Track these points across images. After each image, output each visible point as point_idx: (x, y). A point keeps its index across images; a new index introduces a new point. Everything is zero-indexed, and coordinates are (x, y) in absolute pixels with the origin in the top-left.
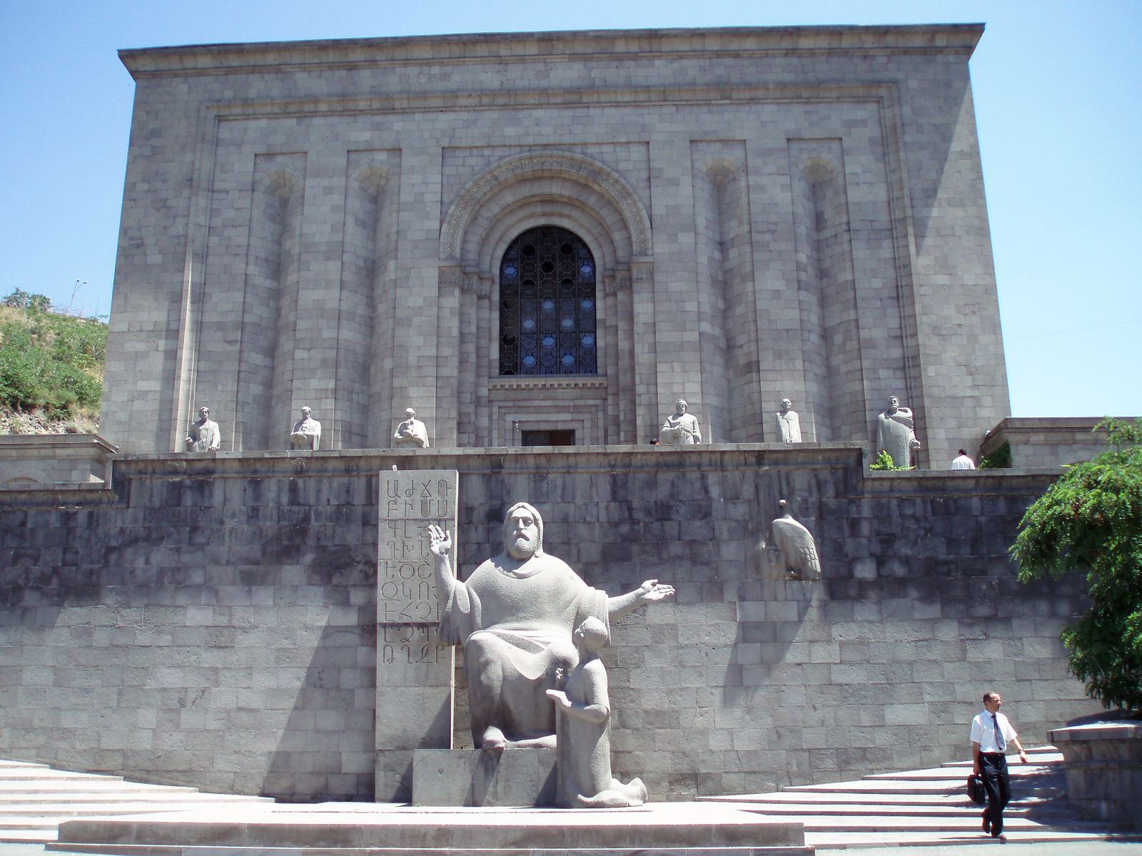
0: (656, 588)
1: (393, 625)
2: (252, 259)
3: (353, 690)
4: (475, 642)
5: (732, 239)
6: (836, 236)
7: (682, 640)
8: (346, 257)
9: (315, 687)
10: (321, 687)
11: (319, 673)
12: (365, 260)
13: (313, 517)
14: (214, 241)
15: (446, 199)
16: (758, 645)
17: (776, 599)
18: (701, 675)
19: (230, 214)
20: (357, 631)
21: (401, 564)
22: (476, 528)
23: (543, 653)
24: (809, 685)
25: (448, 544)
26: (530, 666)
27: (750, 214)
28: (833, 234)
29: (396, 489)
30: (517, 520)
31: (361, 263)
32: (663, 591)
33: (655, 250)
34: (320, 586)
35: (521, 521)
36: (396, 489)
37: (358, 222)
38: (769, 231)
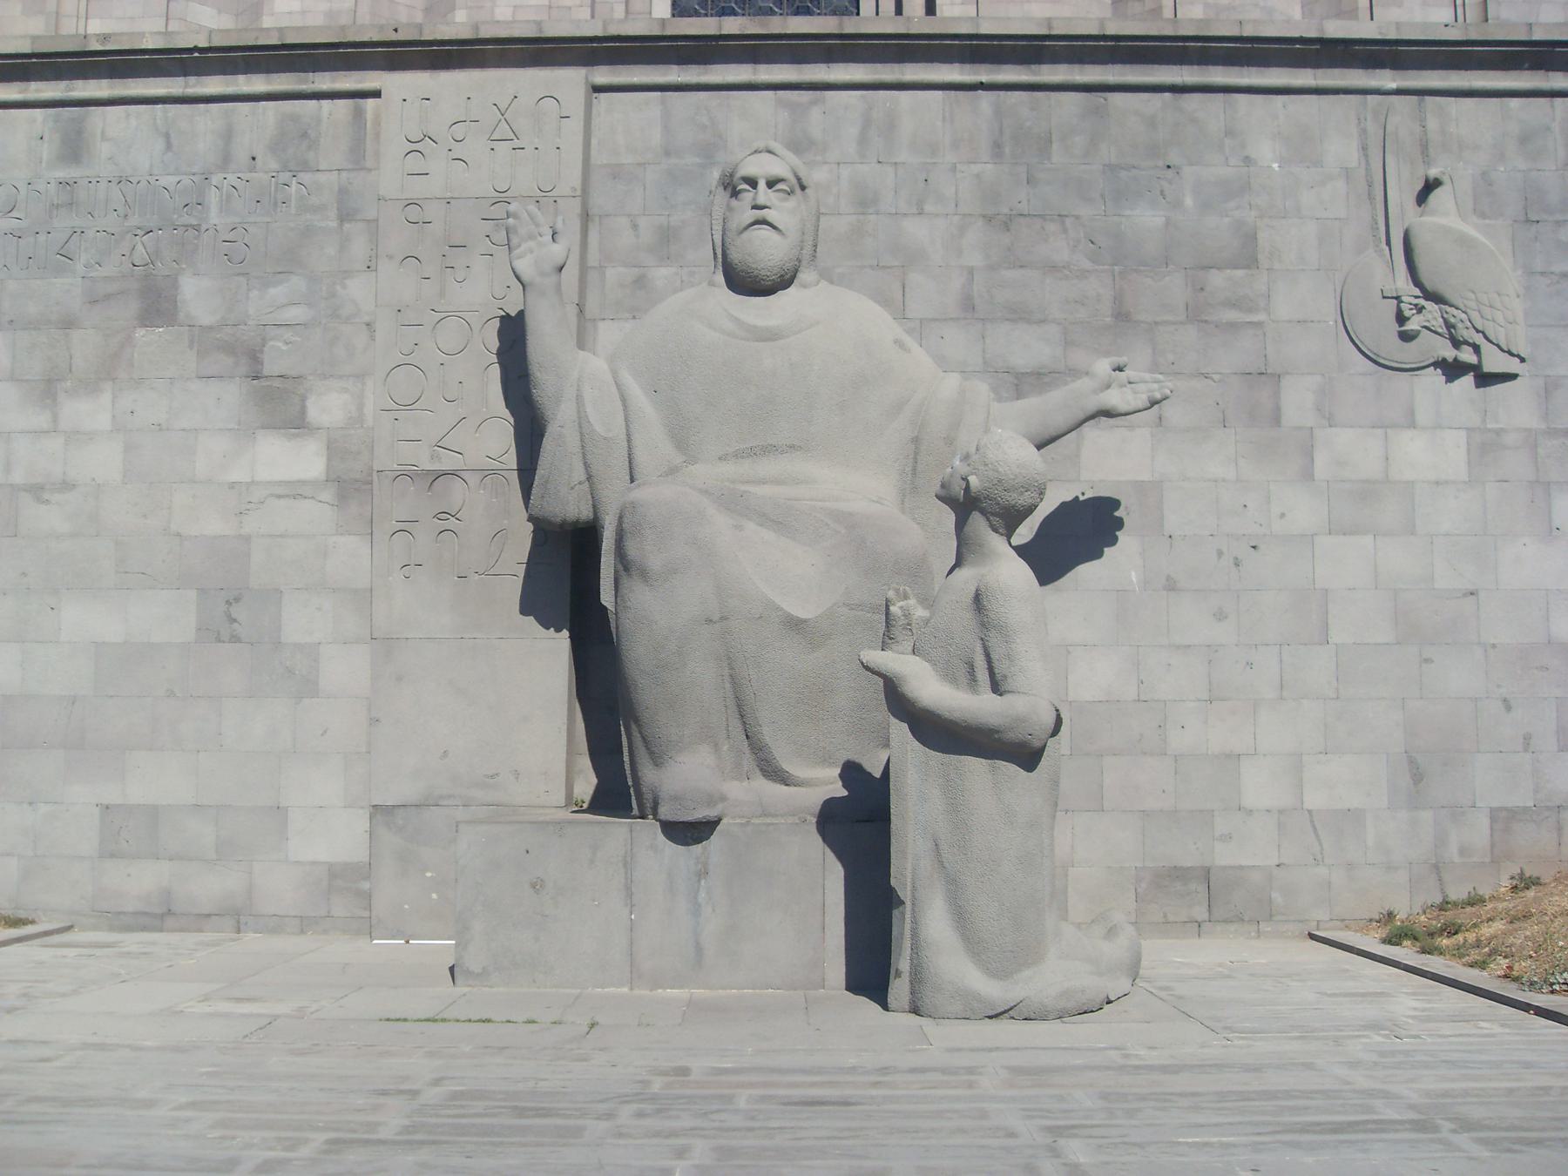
1: (409, 474)
4: (633, 505)
9: (219, 640)
10: (235, 639)
11: (228, 602)
13: (213, 198)
16: (1368, 539)
17: (1412, 425)
20: (328, 495)
24: (1494, 646)
25: (557, 251)
30: (753, 183)
32: (1142, 387)
35: (762, 185)
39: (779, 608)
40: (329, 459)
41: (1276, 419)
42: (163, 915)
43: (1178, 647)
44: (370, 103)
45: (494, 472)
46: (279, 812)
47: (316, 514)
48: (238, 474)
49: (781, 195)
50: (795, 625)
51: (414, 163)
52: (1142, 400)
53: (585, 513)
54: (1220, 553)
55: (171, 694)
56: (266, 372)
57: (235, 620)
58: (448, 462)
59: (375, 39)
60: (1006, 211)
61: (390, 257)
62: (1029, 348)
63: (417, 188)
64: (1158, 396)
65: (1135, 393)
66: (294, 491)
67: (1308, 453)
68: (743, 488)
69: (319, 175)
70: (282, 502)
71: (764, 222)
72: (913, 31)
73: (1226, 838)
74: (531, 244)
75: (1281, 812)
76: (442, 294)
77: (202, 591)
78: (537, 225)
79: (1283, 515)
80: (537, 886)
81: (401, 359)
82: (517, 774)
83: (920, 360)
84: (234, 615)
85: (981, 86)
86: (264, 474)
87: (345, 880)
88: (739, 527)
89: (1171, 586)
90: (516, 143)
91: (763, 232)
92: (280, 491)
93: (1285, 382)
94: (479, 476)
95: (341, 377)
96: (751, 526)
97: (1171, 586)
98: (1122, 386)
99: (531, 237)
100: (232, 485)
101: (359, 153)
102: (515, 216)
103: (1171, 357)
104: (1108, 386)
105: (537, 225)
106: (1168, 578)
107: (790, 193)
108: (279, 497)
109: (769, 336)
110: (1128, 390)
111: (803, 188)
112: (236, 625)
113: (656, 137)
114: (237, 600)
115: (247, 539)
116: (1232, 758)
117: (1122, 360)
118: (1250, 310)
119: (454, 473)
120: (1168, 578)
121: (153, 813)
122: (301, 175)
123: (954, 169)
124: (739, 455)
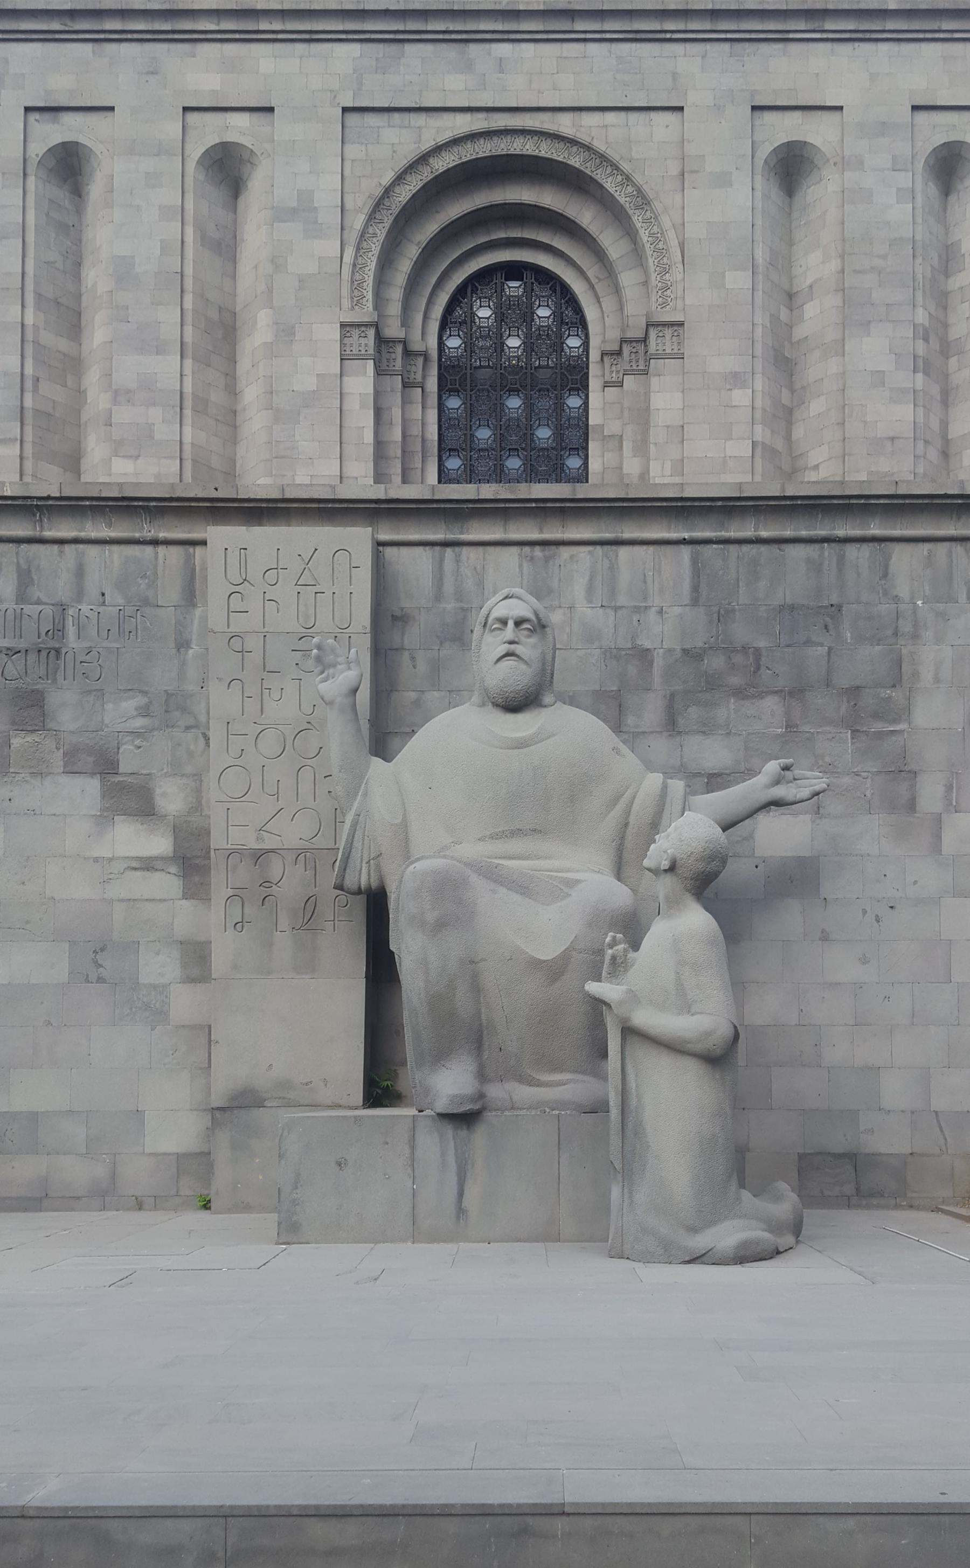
3: (165, 986)
9: (87, 981)
10: (101, 980)
22: (413, 659)
34: (93, 774)
40: (175, 838)
42: (40, 1200)
44: (199, 550)
47: (167, 883)
48: (103, 851)
55: (49, 1023)
56: (120, 771)
57: (101, 966)
60: (701, 644)
62: (713, 753)
66: (147, 865)
67: (938, 837)
68: (497, 861)
70: (138, 873)
77: (72, 943)
83: (629, 761)
85: (684, 542)
86: (122, 851)
92: (134, 864)
95: (182, 775)
100: (96, 860)
101: (191, 594)
103: (828, 759)
108: (135, 869)
112: (101, 969)
114: (102, 950)
118: (895, 721)
121: (34, 1117)
123: (661, 612)
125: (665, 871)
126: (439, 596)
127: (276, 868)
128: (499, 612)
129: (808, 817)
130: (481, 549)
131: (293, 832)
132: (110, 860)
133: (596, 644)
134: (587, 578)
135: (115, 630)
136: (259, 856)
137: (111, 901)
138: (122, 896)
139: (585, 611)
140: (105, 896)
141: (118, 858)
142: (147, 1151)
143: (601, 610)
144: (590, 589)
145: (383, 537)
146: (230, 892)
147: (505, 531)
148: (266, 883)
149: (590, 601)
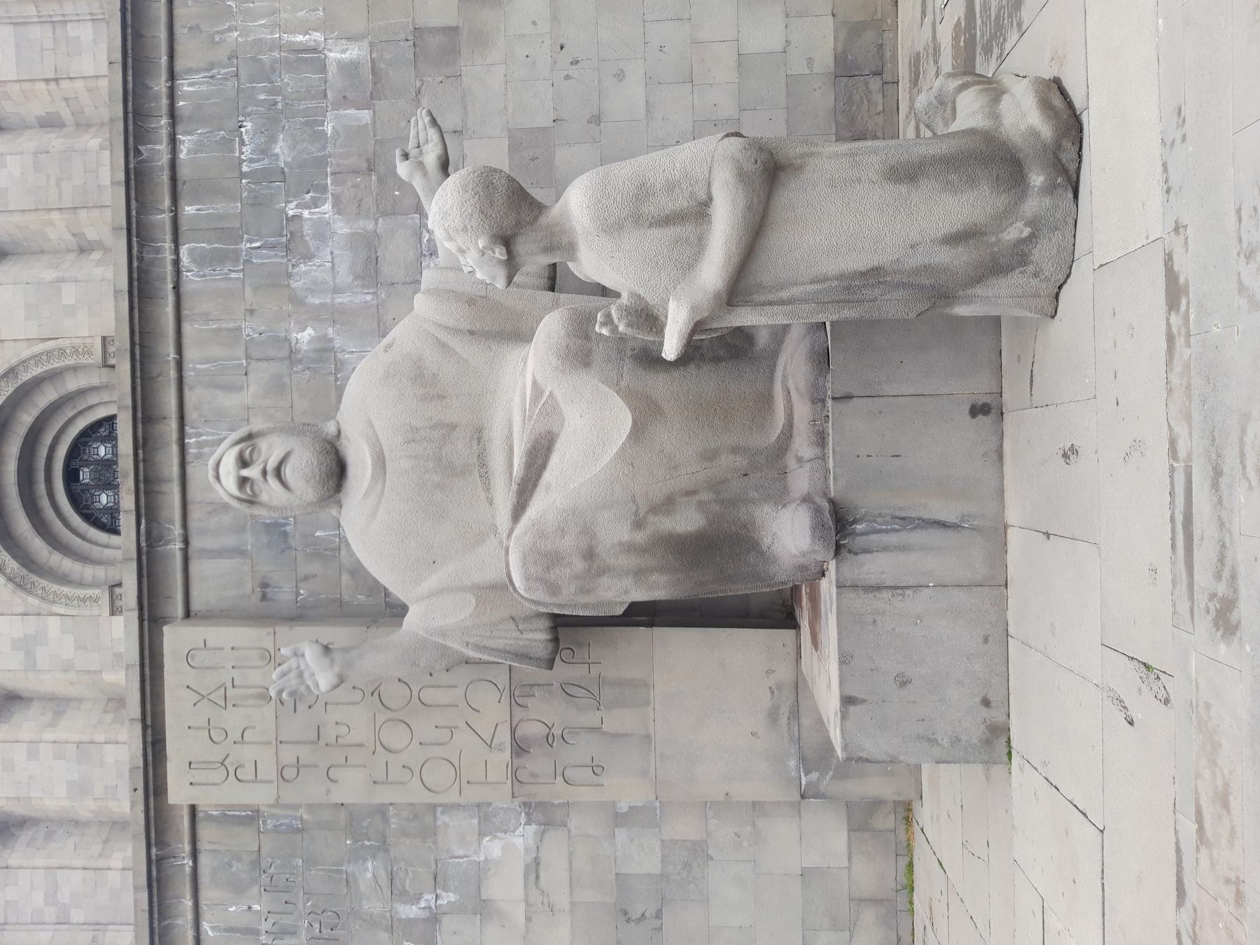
0: (413, 152)
2: (101, 863)
5: (74, 235)
6: (66, 99)
7: (543, 120)
8: (100, 738)
11: (628, 921)
12: (105, 711)
14: (77, 916)
15: (21, 609)
18: (620, 75)
19: (38, 898)
21: (379, 748)
23: (557, 393)
25: (310, 654)
26: (594, 431)
27: (37, 210)
28: (64, 104)
29: (206, 765)
30: (243, 481)
31: (109, 717)
33: (87, 334)
36: (206, 765)
37: (52, 725)
38: (58, 185)
39: (623, 449)
41: (452, 31)
43: (648, 111)
45: (512, 695)
46: (805, 873)
49: (255, 456)
50: (638, 432)
51: (246, 773)
52: (433, 134)
53: (545, 623)
54: (568, 77)
57: (643, 915)
58: (504, 736)
59: (143, 808)
61: (328, 792)
63: (268, 770)
64: (427, 119)
65: (427, 142)
69: (263, 851)
70: (542, 874)
71: (278, 472)
72: (128, 345)
73: (810, 62)
74: (306, 675)
75: (787, 16)
76: (361, 745)
78: (290, 670)
79: (534, 23)
80: (904, 682)
81: (416, 780)
82: (769, 672)
84: (639, 916)
85: (177, 288)
86: (519, 892)
87: (861, 818)
88: (548, 488)
89: (596, 119)
90: (229, 685)
91: (288, 471)
93: (420, 22)
94: (516, 710)
96: (548, 476)
97: (596, 119)
98: (421, 153)
99: (301, 675)
100: (529, 919)
102: (280, 692)
103: (403, 124)
104: (421, 165)
105: (290, 670)
106: (589, 122)
107: (254, 448)
108: (537, 877)
109: (380, 462)
110: (424, 149)
111: (250, 437)
113: (227, 564)
115: (573, 904)
116: (742, 60)
117: (398, 152)
119: (513, 732)
120: (589, 122)
122: (263, 865)
124: (487, 487)
125: (509, 252)
126: (239, 552)
127: (531, 729)
128: (230, 482)
129: (466, 143)
130: (190, 507)
131: (492, 709)
132: (528, 904)
133: (287, 380)
134: (217, 391)
135: (286, 897)
136: (520, 748)
137: (573, 904)
138: (567, 892)
139: (252, 392)
140: (568, 909)
141: (526, 895)
142: (846, 864)
143: (250, 376)
144: (230, 388)
145: (180, 611)
146: (560, 779)
147: (170, 480)
148: (548, 739)
149: (241, 388)
